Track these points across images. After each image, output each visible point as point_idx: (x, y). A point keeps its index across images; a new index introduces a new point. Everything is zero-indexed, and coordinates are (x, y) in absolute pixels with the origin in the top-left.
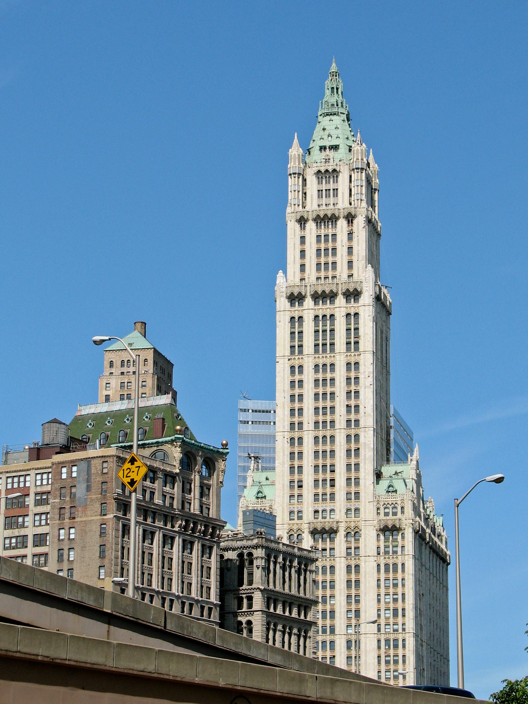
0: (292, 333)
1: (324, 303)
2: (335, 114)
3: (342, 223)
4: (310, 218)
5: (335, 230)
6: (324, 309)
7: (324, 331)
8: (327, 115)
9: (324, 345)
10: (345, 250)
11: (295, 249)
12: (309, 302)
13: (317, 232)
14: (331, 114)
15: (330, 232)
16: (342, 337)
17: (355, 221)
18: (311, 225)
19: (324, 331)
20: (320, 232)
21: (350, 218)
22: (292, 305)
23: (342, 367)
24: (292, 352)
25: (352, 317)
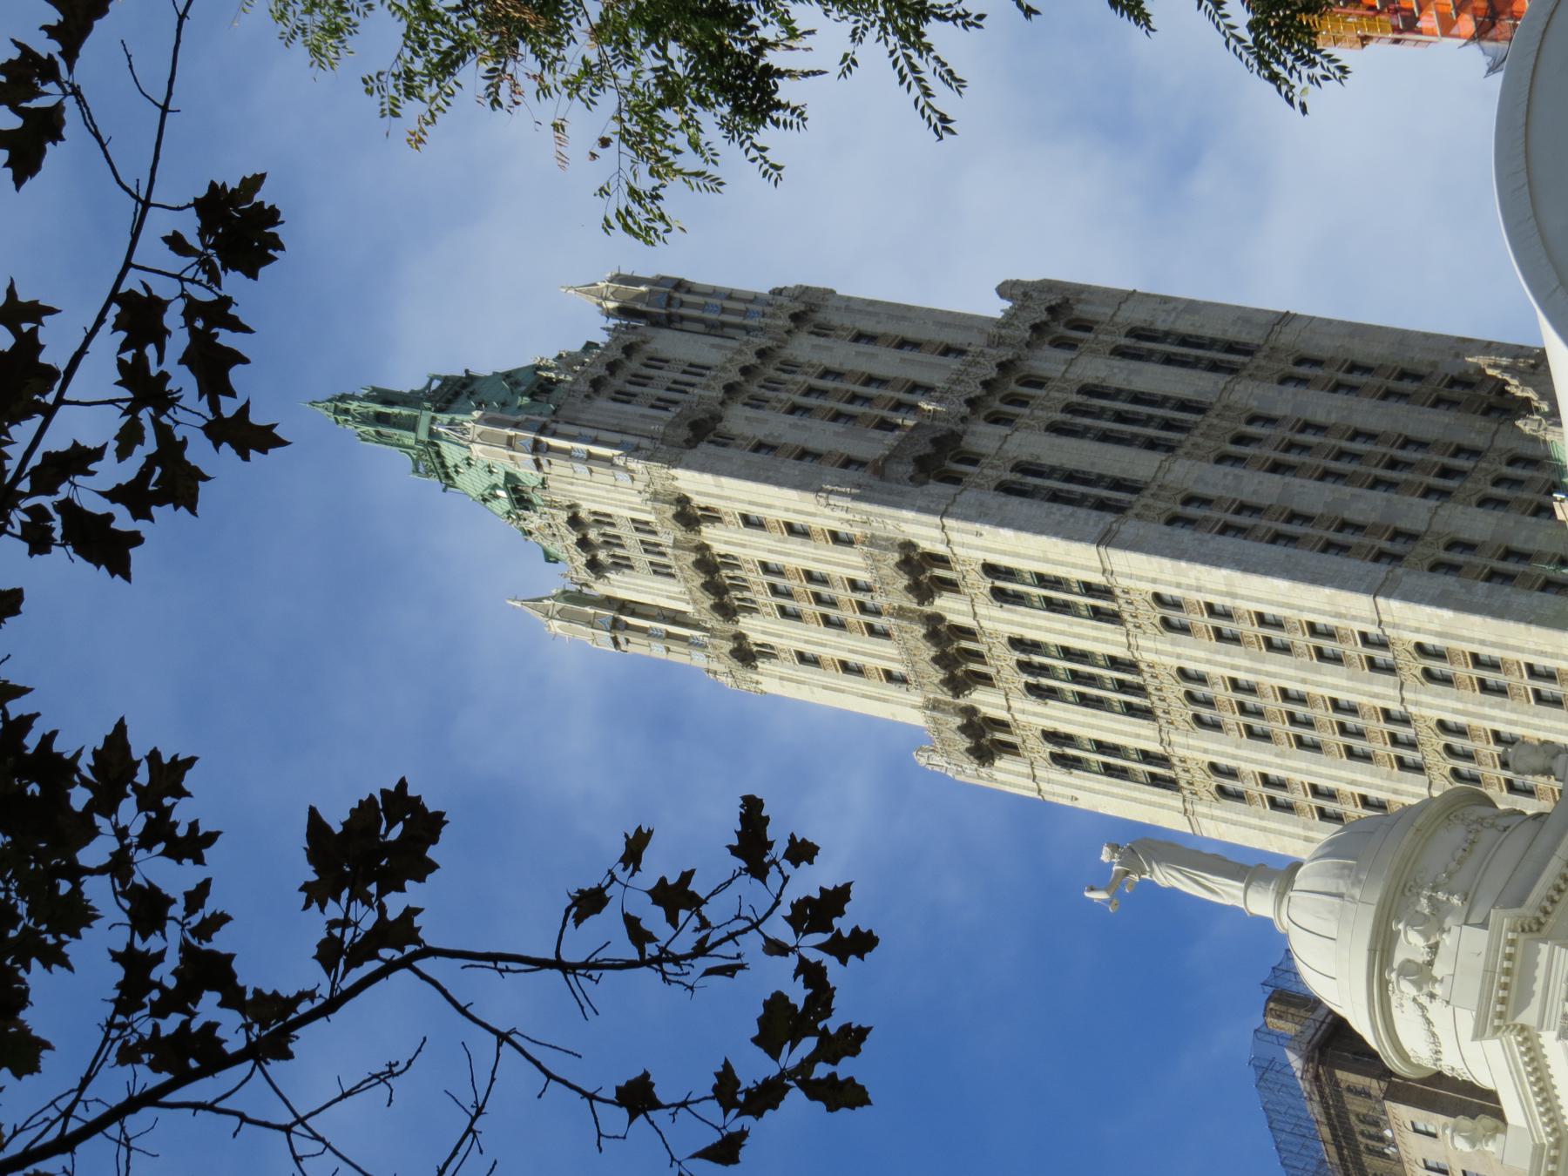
0: (1109, 770)
1: (978, 657)
2: (439, 455)
3: (717, 538)
4: (730, 628)
5: (747, 562)
6: (1003, 662)
7: (1075, 677)
8: (448, 476)
9: (1122, 686)
10: (795, 545)
11: (843, 691)
12: (986, 701)
13: (769, 614)
14: (443, 465)
15: (758, 580)
16: (1077, 630)
17: (698, 500)
18: (755, 628)
19: (1075, 677)
20: (765, 605)
21: (689, 516)
22: (1011, 749)
23: (1179, 650)
24: (1170, 784)
25: (999, 584)
